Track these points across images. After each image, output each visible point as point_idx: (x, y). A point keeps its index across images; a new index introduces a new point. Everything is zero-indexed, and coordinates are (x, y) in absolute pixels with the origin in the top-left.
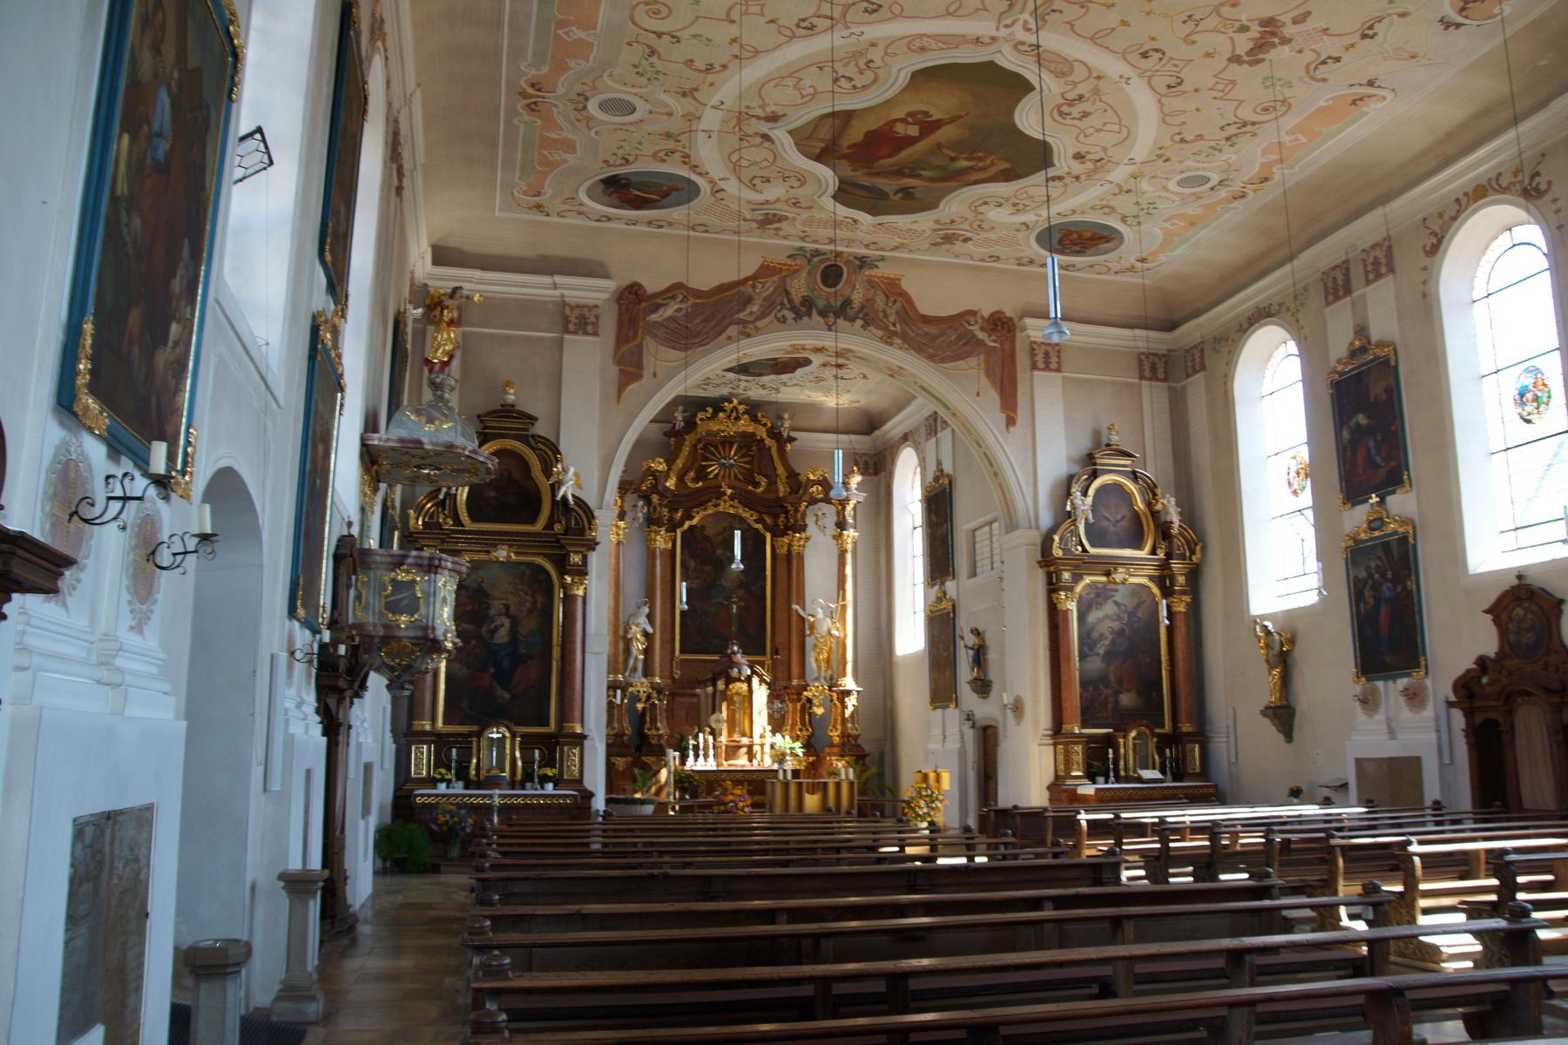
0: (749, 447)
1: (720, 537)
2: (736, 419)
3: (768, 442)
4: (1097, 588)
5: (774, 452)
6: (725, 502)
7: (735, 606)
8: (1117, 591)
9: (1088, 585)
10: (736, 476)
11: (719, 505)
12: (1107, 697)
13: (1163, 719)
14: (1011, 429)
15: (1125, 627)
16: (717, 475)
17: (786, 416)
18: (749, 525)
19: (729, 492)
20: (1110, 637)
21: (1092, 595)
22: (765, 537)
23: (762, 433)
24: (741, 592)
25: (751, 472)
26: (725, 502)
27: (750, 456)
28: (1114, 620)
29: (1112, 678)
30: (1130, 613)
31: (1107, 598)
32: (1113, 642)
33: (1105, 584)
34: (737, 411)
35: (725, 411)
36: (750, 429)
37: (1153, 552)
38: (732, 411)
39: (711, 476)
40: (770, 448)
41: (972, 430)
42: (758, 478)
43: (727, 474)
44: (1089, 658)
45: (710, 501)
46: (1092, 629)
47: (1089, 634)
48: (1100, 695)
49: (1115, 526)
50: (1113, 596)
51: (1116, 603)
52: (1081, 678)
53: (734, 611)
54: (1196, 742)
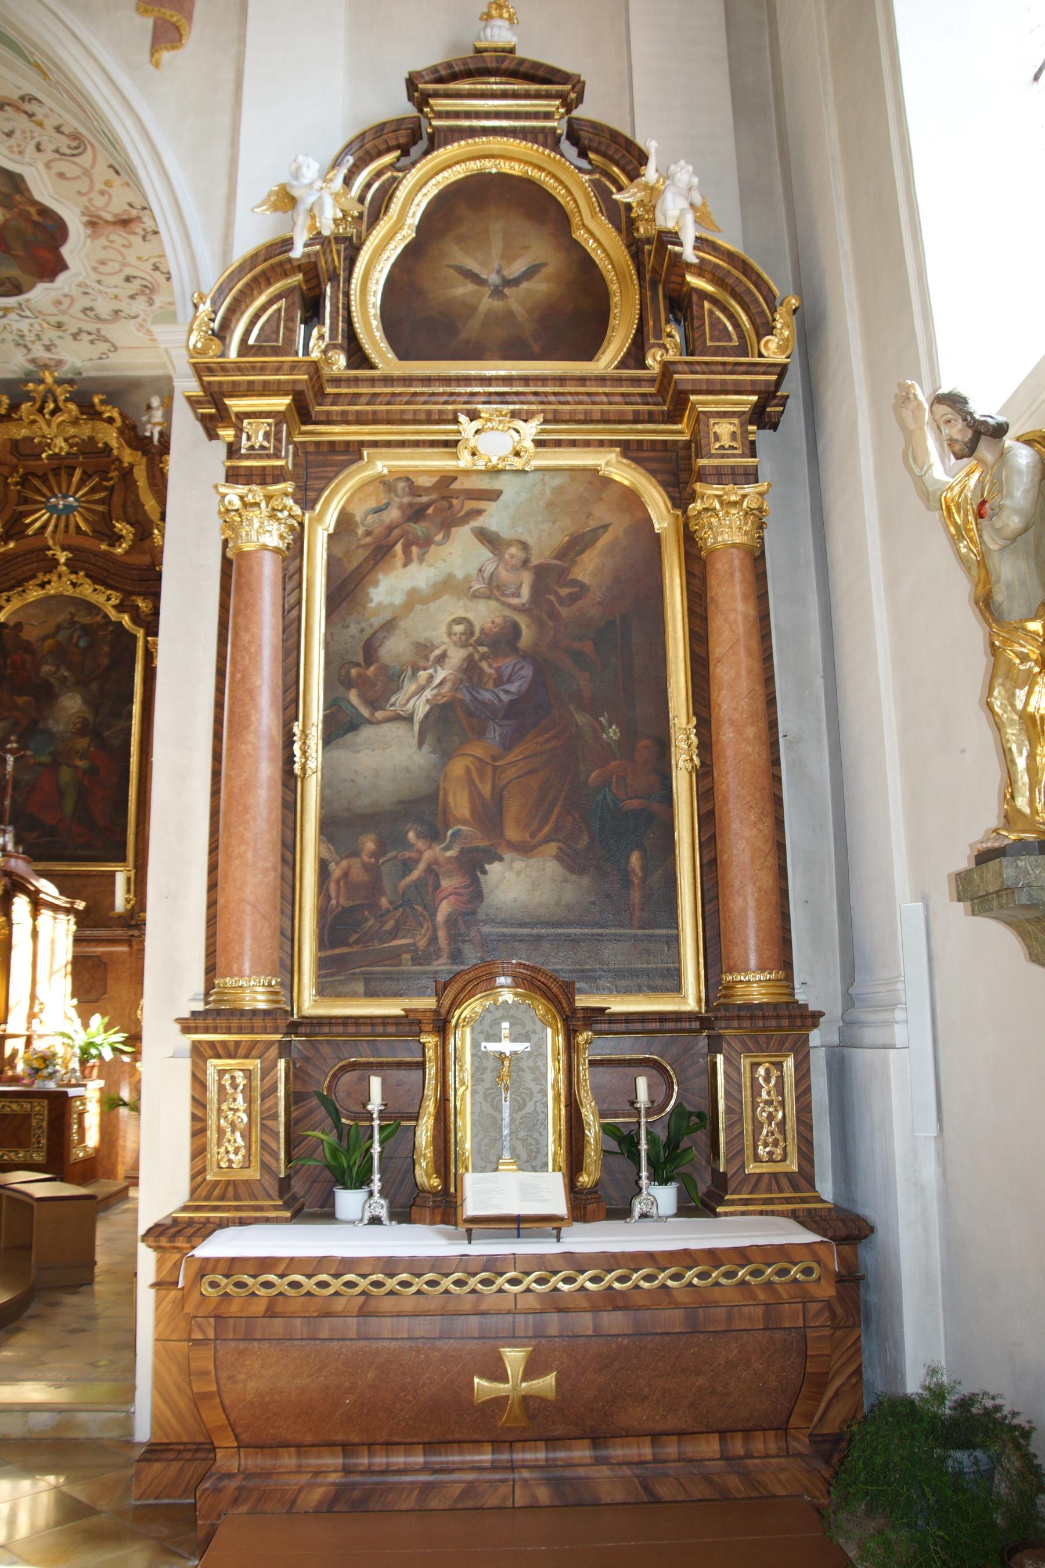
0: (104, 475)
1: (49, 642)
2: (53, 413)
3: (128, 456)
4: (414, 490)
5: (140, 475)
6: (60, 576)
7: (10, 759)
8: (494, 495)
9: (386, 483)
10: (78, 527)
11: (49, 582)
12: (432, 871)
13: (677, 956)
14: (166, 56)
15: (523, 622)
16: (44, 527)
17: (155, 402)
18: (106, 616)
19: (62, 557)
20: (457, 656)
21: (393, 514)
22: (135, 638)
23: (111, 436)
24: (83, 743)
25: (107, 519)
26: (60, 576)
27: (106, 488)
28: (475, 596)
29: (460, 804)
30: (541, 572)
31: (449, 522)
32: (470, 669)
33: (447, 479)
34: (55, 401)
35: (33, 399)
36: (85, 431)
37: (636, 355)
38: (44, 402)
39: (30, 532)
40: (132, 466)
41: (86, 106)
42: (122, 527)
43: (62, 525)
44: (366, 733)
45: (34, 577)
46: (389, 626)
47: (370, 650)
48: (408, 866)
49: (497, 292)
50: (479, 512)
51: (487, 538)
52: (325, 801)
53: (9, 768)
54: (781, 1048)
